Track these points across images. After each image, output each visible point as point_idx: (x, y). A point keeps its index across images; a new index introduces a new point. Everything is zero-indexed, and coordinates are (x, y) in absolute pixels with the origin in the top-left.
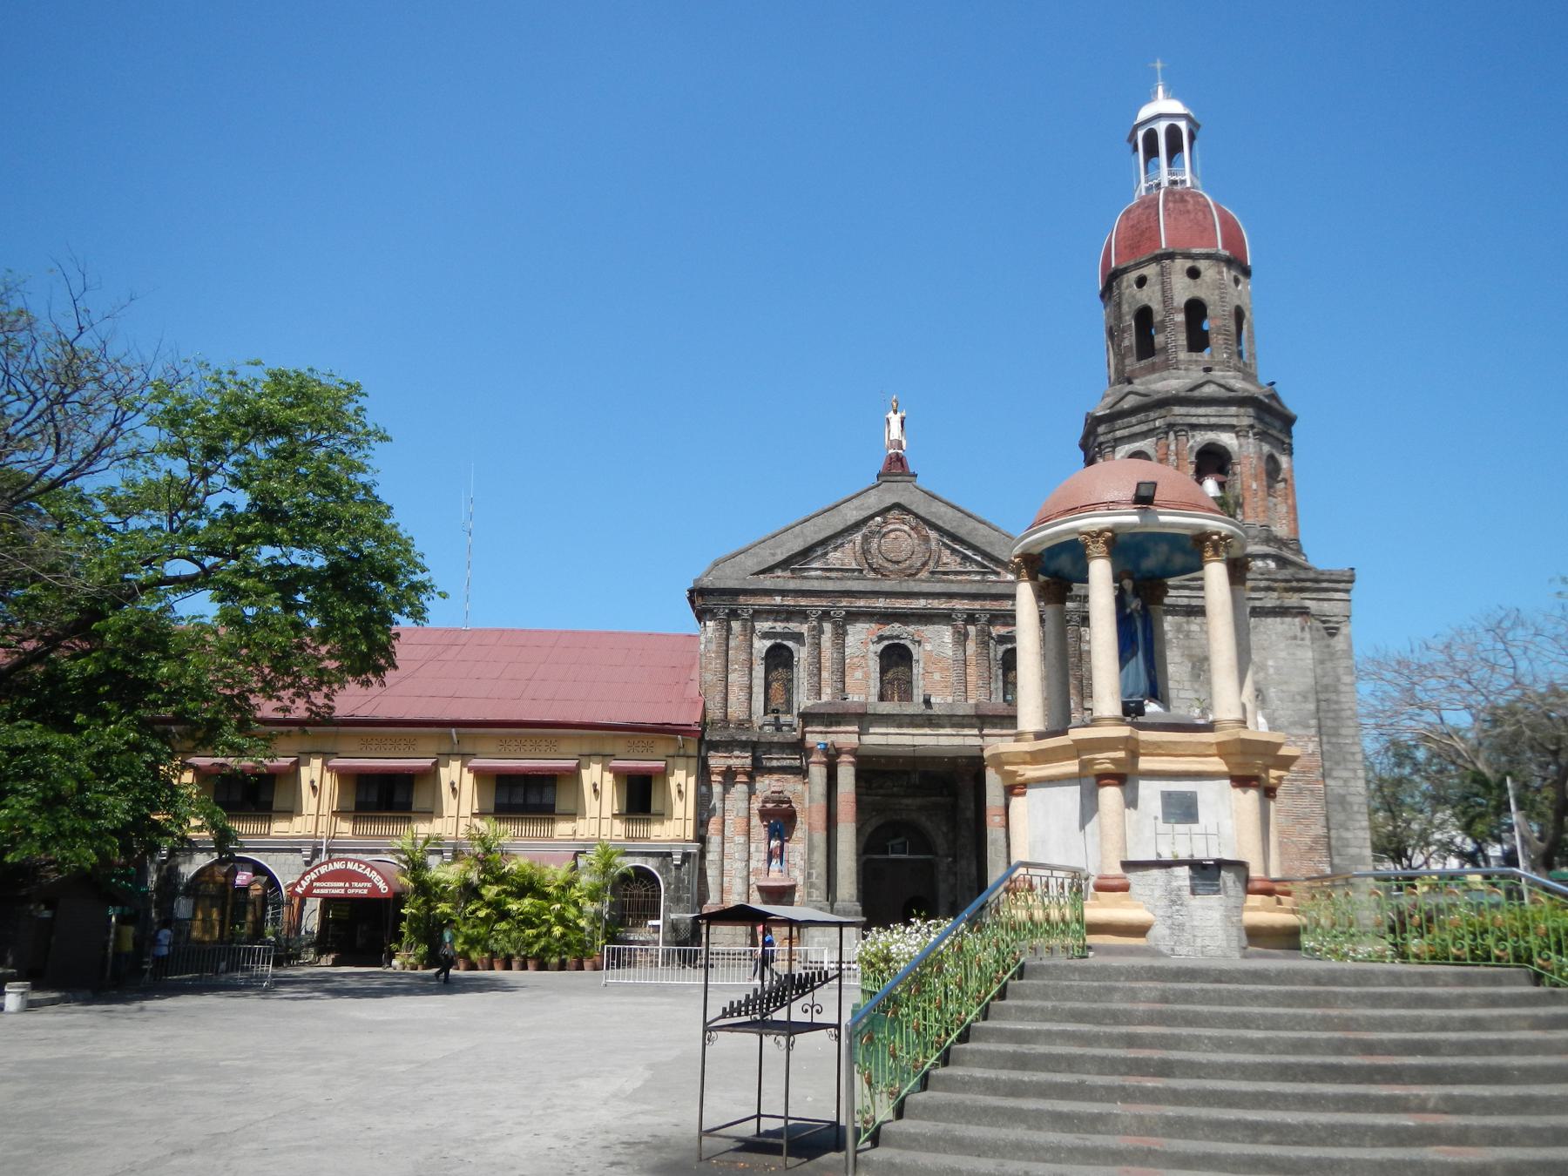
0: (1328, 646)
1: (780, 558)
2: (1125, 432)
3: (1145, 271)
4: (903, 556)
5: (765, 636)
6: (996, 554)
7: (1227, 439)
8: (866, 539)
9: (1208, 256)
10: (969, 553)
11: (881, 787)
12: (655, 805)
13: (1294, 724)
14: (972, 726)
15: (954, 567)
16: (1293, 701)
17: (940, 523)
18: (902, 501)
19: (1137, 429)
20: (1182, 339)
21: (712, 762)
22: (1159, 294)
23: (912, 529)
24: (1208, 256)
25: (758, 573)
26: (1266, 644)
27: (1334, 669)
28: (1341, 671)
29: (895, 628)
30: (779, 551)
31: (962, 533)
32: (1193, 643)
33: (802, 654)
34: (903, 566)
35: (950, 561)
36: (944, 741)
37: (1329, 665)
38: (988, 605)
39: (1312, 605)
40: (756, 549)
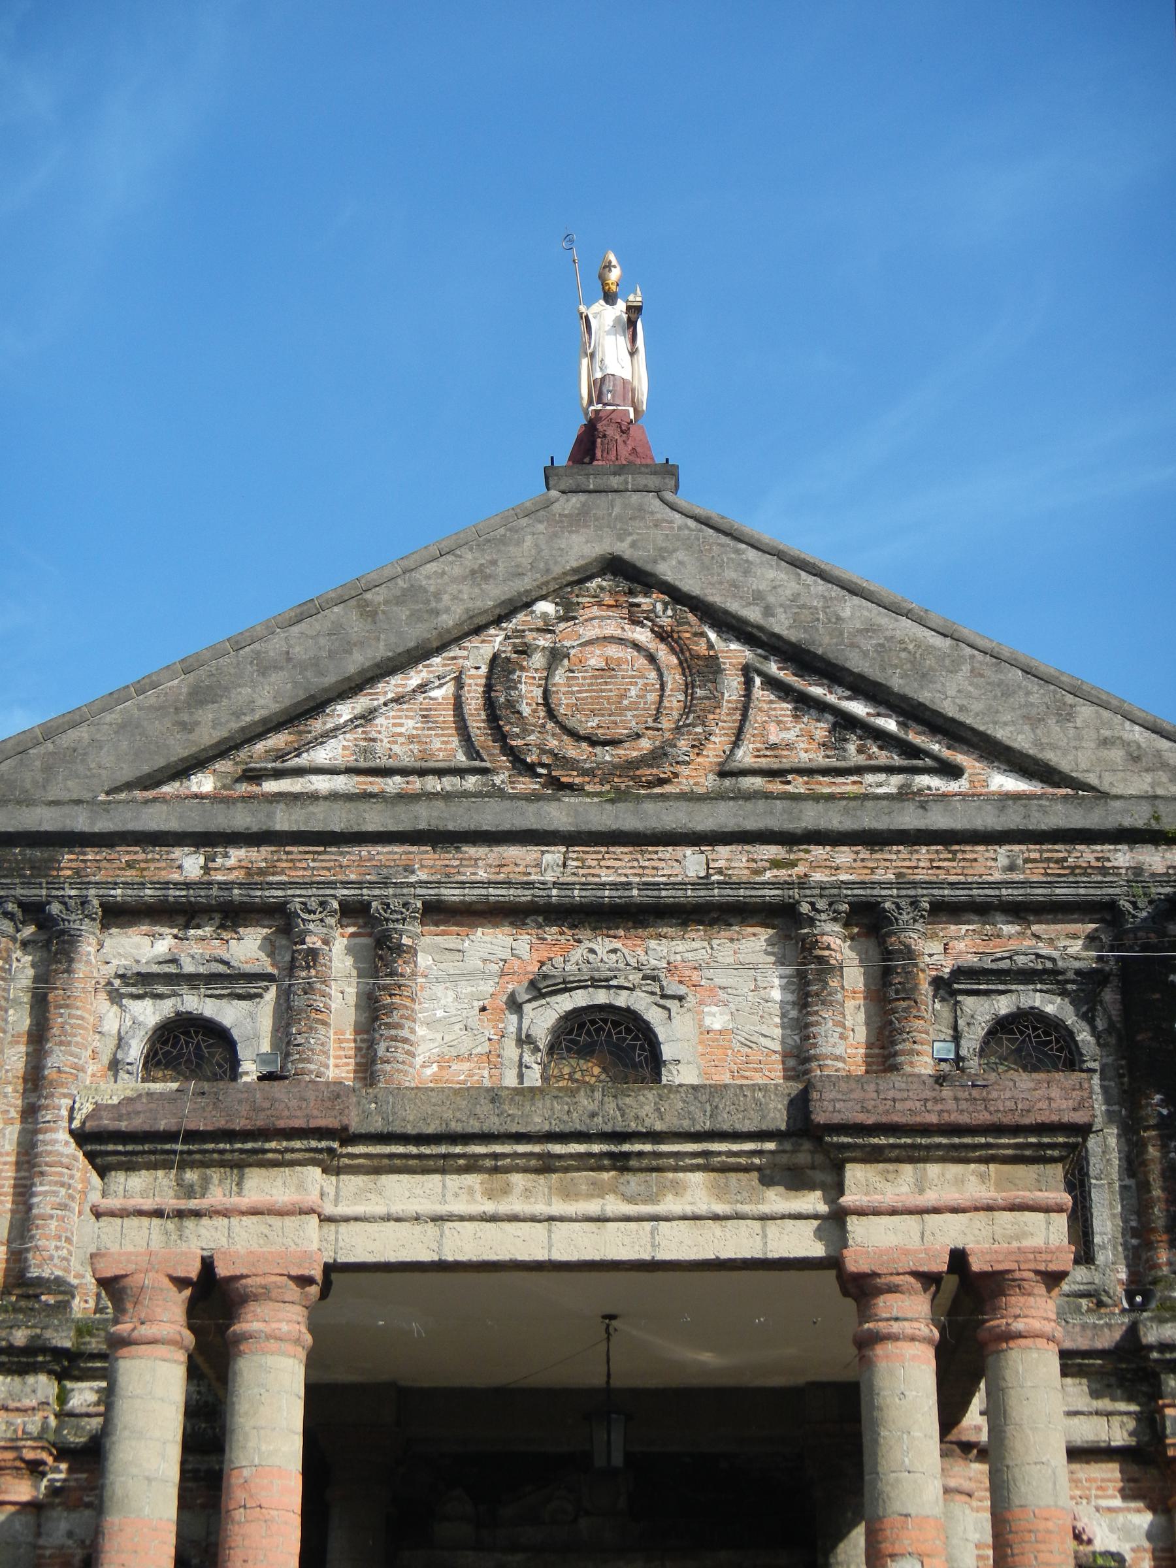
1: (207, 736)
4: (630, 722)
5: (143, 983)
6: (949, 709)
10: (858, 708)
15: (807, 754)
17: (753, 614)
18: (624, 549)
23: (662, 635)
25: (129, 786)
29: (604, 949)
30: (206, 715)
31: (824, 644)
36: (680, 1244)
38: (922, 862)
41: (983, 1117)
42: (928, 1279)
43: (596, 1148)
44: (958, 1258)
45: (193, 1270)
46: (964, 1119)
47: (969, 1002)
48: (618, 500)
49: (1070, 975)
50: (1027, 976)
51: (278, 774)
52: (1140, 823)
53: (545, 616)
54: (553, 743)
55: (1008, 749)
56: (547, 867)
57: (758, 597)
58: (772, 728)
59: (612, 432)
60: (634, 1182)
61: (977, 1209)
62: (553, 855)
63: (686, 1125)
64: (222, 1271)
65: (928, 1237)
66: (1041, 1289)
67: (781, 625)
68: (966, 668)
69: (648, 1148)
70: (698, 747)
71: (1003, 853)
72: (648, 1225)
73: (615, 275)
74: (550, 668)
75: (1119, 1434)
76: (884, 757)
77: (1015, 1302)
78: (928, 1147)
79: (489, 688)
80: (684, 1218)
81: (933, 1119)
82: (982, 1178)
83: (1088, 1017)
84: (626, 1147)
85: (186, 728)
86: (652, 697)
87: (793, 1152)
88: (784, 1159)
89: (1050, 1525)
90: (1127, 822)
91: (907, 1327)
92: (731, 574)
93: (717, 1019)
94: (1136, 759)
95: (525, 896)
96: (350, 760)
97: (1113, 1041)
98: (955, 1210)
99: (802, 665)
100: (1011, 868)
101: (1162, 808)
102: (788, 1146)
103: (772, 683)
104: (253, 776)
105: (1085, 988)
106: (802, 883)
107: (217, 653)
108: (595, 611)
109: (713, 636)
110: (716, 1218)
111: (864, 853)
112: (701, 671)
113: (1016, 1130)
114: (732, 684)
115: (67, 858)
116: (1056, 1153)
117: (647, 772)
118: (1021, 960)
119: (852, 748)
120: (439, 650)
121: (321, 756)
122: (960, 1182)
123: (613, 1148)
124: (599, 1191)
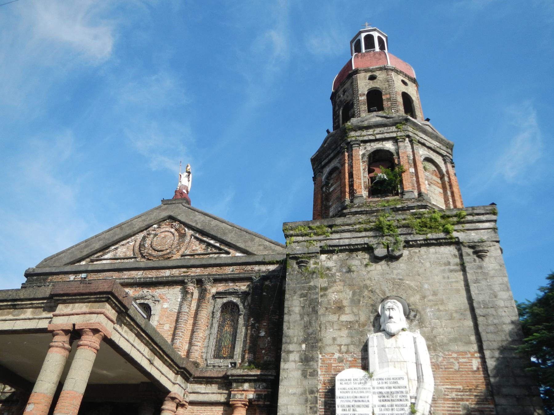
0: (481, 267)
1: (85, 253)
6: (229, 240)
7: (389, 146)
9: (381, 69)
10: (212, 242)
13: (455, 340)
16: (451, 318)
17: (194, 224)
20: (364, 107)
23: (176, 230)
24: (381, 69)
26: (421, 270)
27: (490, 287)
28: (496, 288)
29: (145, 291)
30: (86, 250)
31: (207, 229)
32: (354, 275)
35: (199, 248)
37: (484, 283)
38: (214, 271)
41: (88, 291)
42: (66, 332)
43: (9, 303)
46: (84, 292)
47: (218, 300)
48: (174, 205)
49: (240, 293)
50: (231, 294)
51: (97, 260)
52: (260, 260)
54: (150, 252)
55: (239, 248)
56: (139, 275)
57: (196, 221)
58: (194, 246)
59: (178, 194)
60: (16, 311)
61: (82, 314)
62: (140, 273)
63: (28, 297)
65: (69, 321)
66: (92, 334)
67: (199, 226)
68: (234, 232)
69: (20, 303)
70: (178, 251)
71: (231, 268)
72: (14, 321)
73: (189, 168)
74: (154, 238)
75: (222, 398)
76: (214, 250)
77: (84, 337)
78: (75, 299)
80: (22, 319)
81: (76, 292)
82: (87, 306)
83: (243, 303)
84: (15, 303)
85: (81, 252)
86: (172, 242)
87: (50, 302)
88: (48, 304)
89: (68, 395)
90: (257, 260)
91: (56, 344)
92: (191, 217)
93: (166, 305)
94: (265, 248)
95: (132, 281)
96: (112, 257)
97: (248, 307)
98: (77, 314)
99: (202, 233)
100: (232, 271)
101: (266, 257)
102: (49, 301)
103: (196, 238)
104: (92, 261)
105: (244, 295)
106: (187, 276)
107: (92, 238)
108: (165, 226)
109: (186, 229)
110: (29, 319)
111: (202, 269)
112: (182, 236)
113: (95, 294)
114: (189, 238)
115: (50, 278)
116: (104, 300)
117: (166, 256)
118: (231, 290)
119: (209, 250)
120: (134, 235)
121: (106, 257)
122: (81, 307)
123: (13, 303)
124: (9, 314)
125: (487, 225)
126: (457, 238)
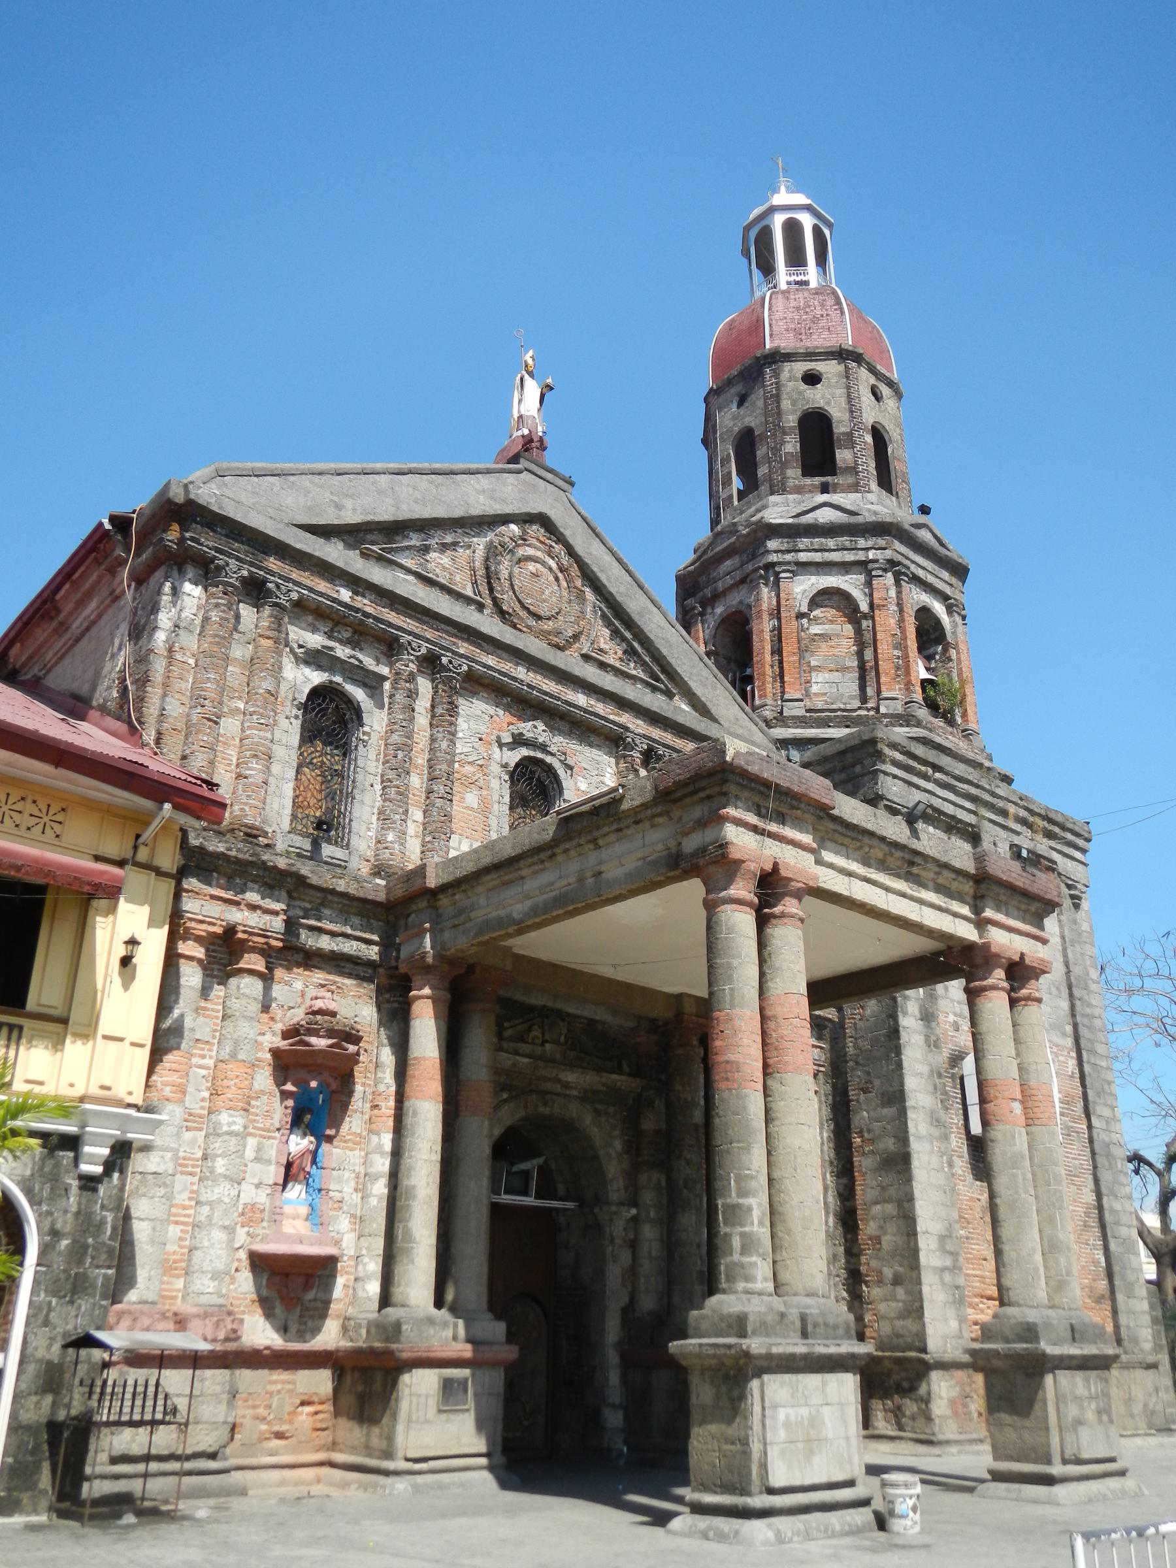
0: (1075, 922)
1: (350, 516)
2: (817, 557)
3: (821, 367)
6: (673, 661)
7: (939, 608)
8: (492, 552)
11: (521, 1039)
12: (44, 990)
14: (959, 897)
15: (611, 660)
17: (603, 577)
19: (836, 557)
21: (190, 905)
22: (843, 400)
30: (349, 504)
33: (376, 721)
34: (549, 625)
35: (613, 653)
39: (1062, 863)
40: (305, 481)
44: (1022, 955)
45: (768, 867)
53: (513, 531)
64: (783, 873)
79: (487, 559)
108: (535, 542)
125: (1078, 855)
126: (1055, 863)
